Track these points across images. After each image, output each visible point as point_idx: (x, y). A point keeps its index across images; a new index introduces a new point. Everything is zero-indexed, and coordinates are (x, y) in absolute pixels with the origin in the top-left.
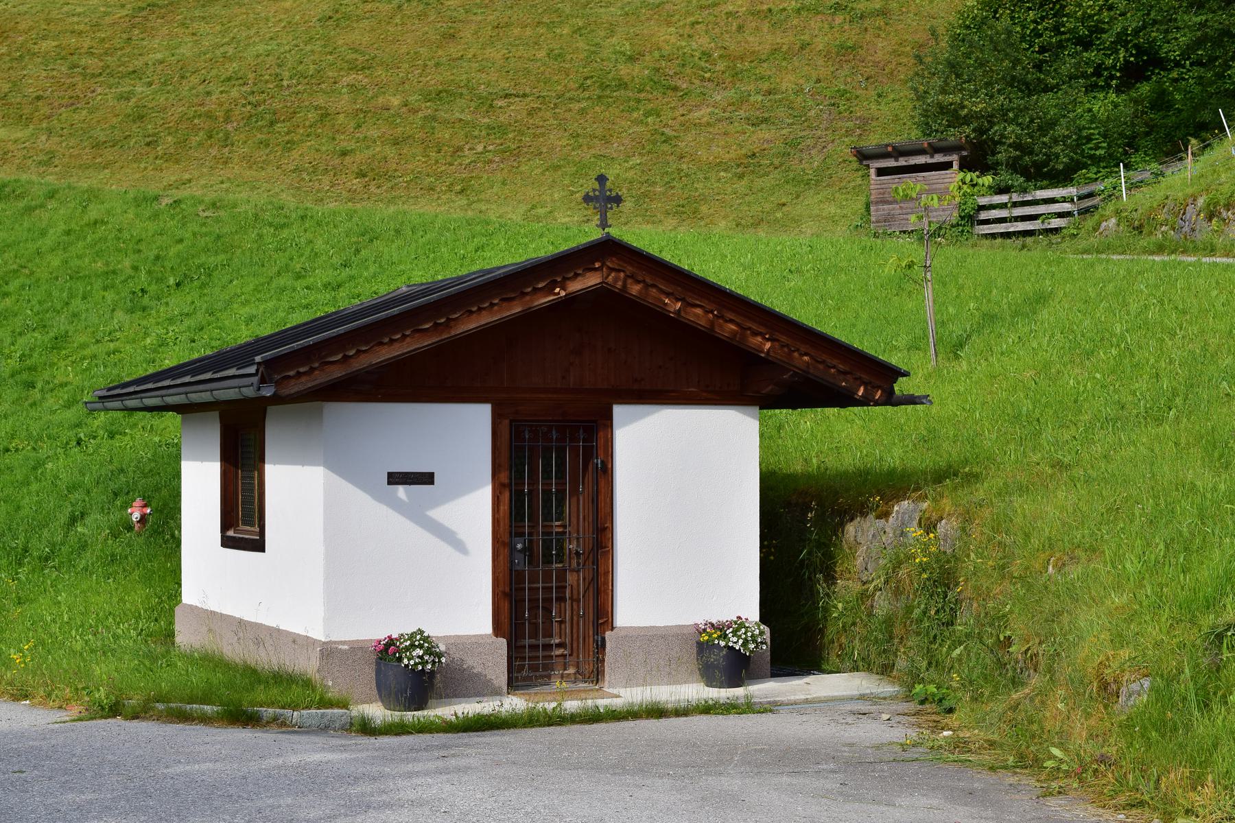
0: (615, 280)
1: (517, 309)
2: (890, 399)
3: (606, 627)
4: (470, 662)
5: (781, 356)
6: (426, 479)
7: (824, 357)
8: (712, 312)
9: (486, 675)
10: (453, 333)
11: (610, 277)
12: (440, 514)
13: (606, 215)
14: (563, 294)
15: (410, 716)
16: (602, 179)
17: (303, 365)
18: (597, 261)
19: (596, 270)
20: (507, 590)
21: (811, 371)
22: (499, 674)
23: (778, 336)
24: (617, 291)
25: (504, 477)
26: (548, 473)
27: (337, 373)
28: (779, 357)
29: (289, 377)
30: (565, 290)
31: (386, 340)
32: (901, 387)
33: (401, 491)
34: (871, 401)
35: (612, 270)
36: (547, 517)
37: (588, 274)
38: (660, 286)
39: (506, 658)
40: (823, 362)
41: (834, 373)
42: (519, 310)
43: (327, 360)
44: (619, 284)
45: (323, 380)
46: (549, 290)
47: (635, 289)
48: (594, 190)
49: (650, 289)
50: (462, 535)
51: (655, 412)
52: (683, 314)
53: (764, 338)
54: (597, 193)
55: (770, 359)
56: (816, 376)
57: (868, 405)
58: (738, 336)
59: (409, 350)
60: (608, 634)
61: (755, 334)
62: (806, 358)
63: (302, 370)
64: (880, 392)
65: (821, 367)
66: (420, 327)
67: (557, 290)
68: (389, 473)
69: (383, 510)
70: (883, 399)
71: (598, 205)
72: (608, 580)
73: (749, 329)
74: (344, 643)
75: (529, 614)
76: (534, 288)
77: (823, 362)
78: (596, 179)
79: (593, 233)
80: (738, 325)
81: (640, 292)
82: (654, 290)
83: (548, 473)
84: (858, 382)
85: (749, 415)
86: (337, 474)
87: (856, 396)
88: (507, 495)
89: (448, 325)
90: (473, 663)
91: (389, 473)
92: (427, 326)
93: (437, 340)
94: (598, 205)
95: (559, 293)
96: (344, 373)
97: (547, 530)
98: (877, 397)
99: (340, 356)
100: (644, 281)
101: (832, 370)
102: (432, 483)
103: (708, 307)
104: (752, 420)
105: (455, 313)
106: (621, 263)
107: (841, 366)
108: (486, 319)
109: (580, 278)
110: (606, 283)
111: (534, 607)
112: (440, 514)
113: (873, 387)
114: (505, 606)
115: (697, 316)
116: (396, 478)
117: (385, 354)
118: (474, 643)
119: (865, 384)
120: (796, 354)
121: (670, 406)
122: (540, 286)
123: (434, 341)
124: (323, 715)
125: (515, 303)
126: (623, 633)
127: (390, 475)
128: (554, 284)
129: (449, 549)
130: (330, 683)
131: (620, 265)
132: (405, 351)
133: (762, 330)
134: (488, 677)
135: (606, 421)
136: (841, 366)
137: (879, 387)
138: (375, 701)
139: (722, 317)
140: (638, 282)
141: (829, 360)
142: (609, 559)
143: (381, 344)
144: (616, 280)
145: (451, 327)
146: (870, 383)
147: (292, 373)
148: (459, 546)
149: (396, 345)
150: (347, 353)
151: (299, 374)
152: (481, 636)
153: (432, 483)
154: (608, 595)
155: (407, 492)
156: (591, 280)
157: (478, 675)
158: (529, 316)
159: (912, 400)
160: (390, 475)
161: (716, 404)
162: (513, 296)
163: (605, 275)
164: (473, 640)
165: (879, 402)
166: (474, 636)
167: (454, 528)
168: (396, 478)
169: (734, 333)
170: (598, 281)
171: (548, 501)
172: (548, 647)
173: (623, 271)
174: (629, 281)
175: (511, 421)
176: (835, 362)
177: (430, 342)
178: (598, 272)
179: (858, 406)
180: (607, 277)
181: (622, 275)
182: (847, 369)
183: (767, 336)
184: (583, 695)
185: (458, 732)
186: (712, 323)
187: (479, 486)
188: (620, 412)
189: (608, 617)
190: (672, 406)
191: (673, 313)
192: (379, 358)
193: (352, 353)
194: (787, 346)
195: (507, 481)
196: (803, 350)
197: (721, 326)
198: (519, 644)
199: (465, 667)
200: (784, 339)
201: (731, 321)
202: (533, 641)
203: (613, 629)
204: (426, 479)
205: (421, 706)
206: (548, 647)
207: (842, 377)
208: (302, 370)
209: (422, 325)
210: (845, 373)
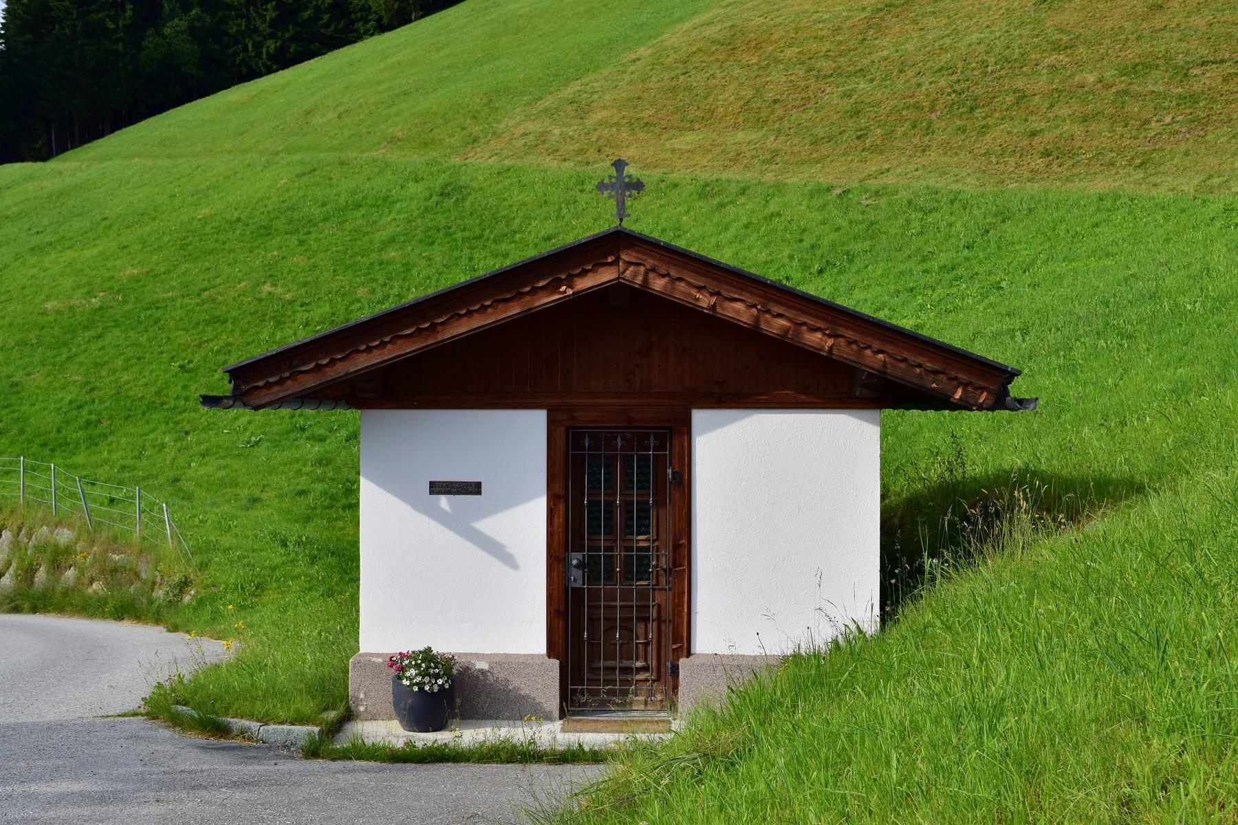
0: (634, 276)
1: (514, 310)
2: (1000, 401)
3: (680, 653)
4: (515, 683)
5: (849, 354)
6: (474, 488)
7: (905, 354)
8: (754, 306)
9: (534, 699)
10: (440, 338)
11: (628, 272)
12: (485, 526)
13: (624, 203)
14: (570, 292)
15: (426, 739)
16: (619, 165)
17: (272, 375)
18: (610, 255)
19: (610, 264)
20: (562, 608)
21: (889, 371)
22: (550, 698)
23: (842, 331)
24: (637, 286)
25: (559, 489)
26: (627, 484)
27: (310, 382)
28: (845, 356)
29: (258, 388)
30: (572, 288)
31: (363, 347)
32: (1016, 389)
33: (444, 501)
34: (973, 405)
35: (631, 263)
36: (628, 529)
37: (601, 270)
38: (688, 279)
39: (558, 681)
40: (905, 360)
41: (917, 371)
42: (518, 311)
43: (299, 369)
44: (639, 280)
45: (296, 390)
46: (553, 287)
47: (658, 284)
48: (610, 177)
49: (677, 283)
50: (512, 549)
51: (745, 417)
52: (719, 310)
53: (825, 334)
54: (614, 180)
55: (834, 357)
56: (894, 376)
57: (971, 410)
58: (791, 332)
59: (390, 357)
60: (683, 662)
61: (814, 330)
62: (881, 356)
63: (271, 380)
64: (985, 394)
65: (902, 365)
66: (401, 333)
67: (564, 288)
68: (431, 483)
69: (424, 521)
70: (990, 402)
71: (613, 193)
72: (683, 601)
73: (805, 324)
74: (378, 655)
75: (620, 635)
76: (533, 287)
77: (905, 360)
78: (612, 165)
79: (605, 223)
80: (789, 319)
81: (665, 287)
82: (683, 284)
83: (610, 482)
84: (955, 383)
85: (867, 421)
86: (374, 483)
87: (952, 400)
88: (562, 507)
89: (433, 328)
90: (523, 685)
91: (431, 483)
92: (408, 332)
93: (421, 345)
94: (613, 193)
95: (565, 292)
96: (318, 382)
97: (626, 544)
98: (981, 401)
99: (312, 365)
100: (668, 275)
101: (918, 370)
102: (479, 493)
103: (751, 301)
104: (871, 426)
105: (441, 317)
106: (640, 256)
107: (929, 365)
108: (478, 322)
109: (590, 274)
110: (623, 279)
111: (610, 630)
112: (487, 526)
113: (976, 389)
114: (560, 624)
115: (738, 312)
116: (438, 488)
117: (363, 361)
118: (523, 663)
119: (965, 385)
120: (868, 352)
121: (786, 411)
122: (540, 284)
123: (418, 347)
124: (289, 732)
125: (512, 304)
126: (700, 661)
127: (432, 484)
128: (559, 283)
129: (497, 564)
130: (362, 696)
131: (639, 259)
132: (386, 358)
133: (821, 325)
134: (537, 700)
135: (682, 432)
136: (929, 365)
137: (983, 389)
138: (390, 718)
139: (768, 311)
140: (663, 276)
141: (913, 358)
142: (684, 578)
143: (359, 351)
144: (635, 275)
145: (438, 332)
146: (970, 383)
147: (261, 383)
148: (509, 560)
149: (376, 352)
150: (320, 362)
151: (268, 386)
152: (532, 656)
153: (479, 493)
154: (682, 617)
155: (450, 503)
156: (605, 276)
157: (525, 697)
158: (530, 319)
159: (1021, 403)
160: (432, 484)
161: (823, 408)
162: (509, 296)
163: (621, 269)
164: (521, 660)
165: (984, 406)
166: (524, 655)
167: (503, 542)
168: (438, 488)
169: (787, 330)
170: (614, 276)
171: (594, 519)
172: (627, 670)
173: (643, 265)
174: (651, 275)
175: (568, 429)
176: (920, 360)
177: (414, 348)
178: (613, 267)
179: (923, 408)
180: (624, 272)
181: (642, 269)
182: (937, 367)
183: (827, 332)
184: (635, 727)
185: (397, 762)
186: (757, 320)
187: (525, 497)
188: (699, 417)
189: (682, 642)
190: (767, 411)
191: (706, 309)
192: (357, 366)
193: (325, 361)
194: (855, 342)
195: (562, 492)
196: (876, 345)
197: (767, 322)
198: (594, 666)
199: (510, 687)
200: (850, 334)
201: (780, 316)
202: (610, 663)
203: (689, 654)
204: (474, 488)
205: (439, 728)
206: (627, 670)
207: (931, 377)
208: (271, 380)
209: (402, 331)
210: (935, 372)
